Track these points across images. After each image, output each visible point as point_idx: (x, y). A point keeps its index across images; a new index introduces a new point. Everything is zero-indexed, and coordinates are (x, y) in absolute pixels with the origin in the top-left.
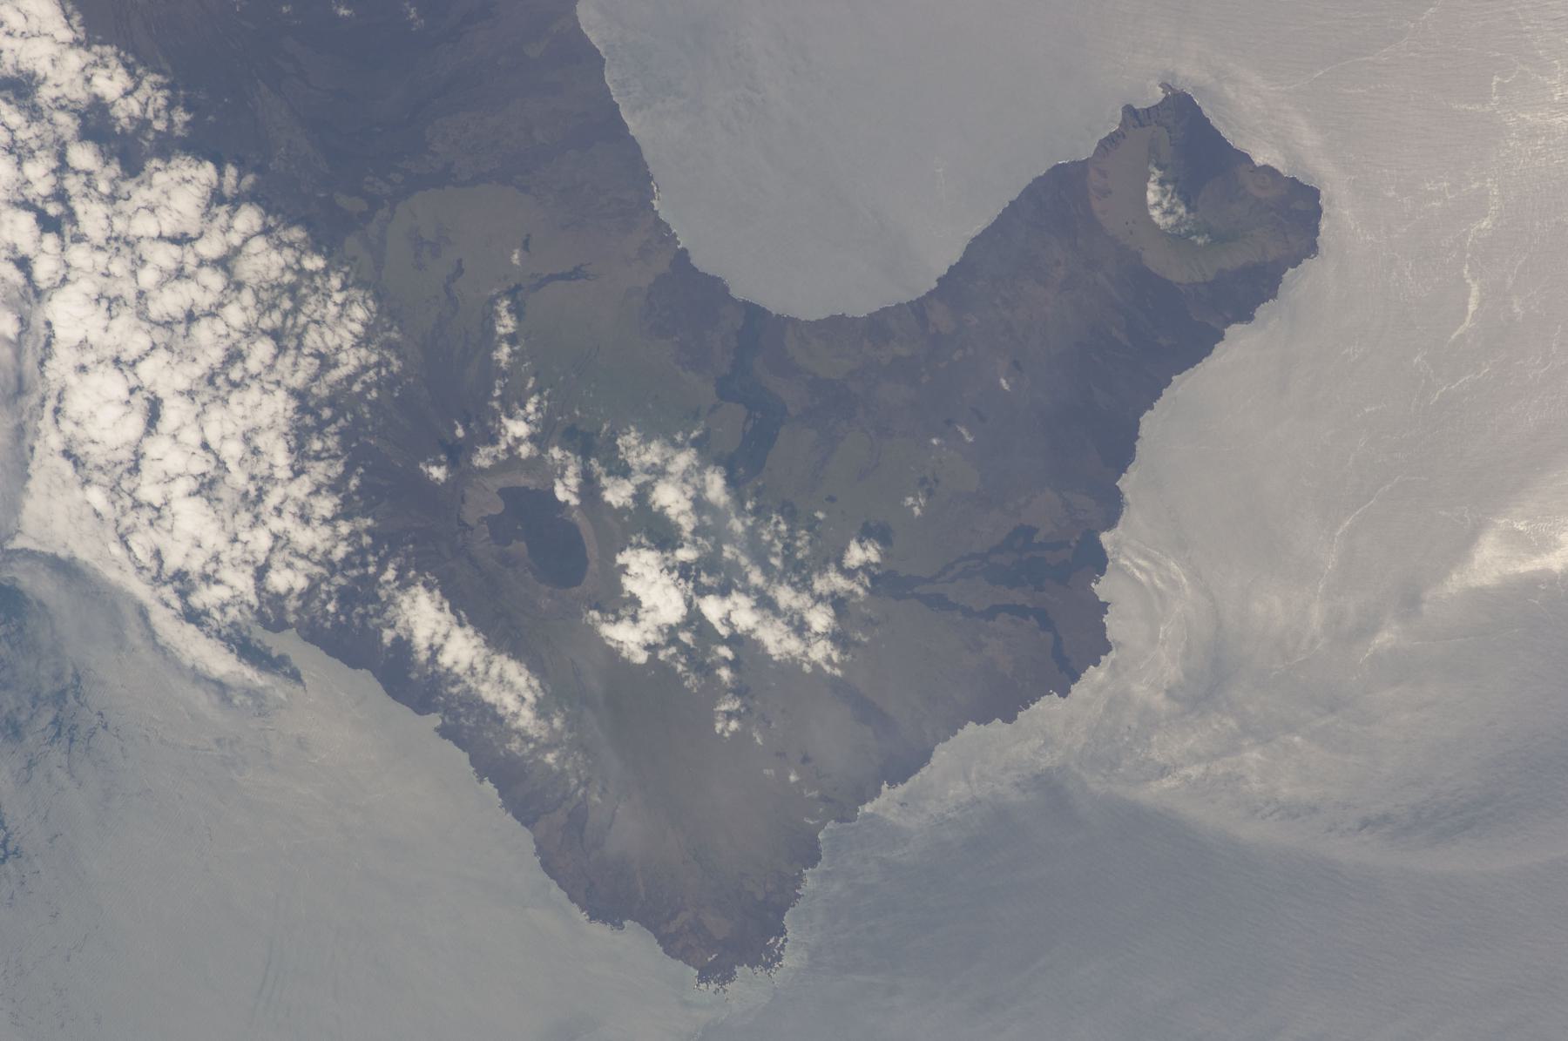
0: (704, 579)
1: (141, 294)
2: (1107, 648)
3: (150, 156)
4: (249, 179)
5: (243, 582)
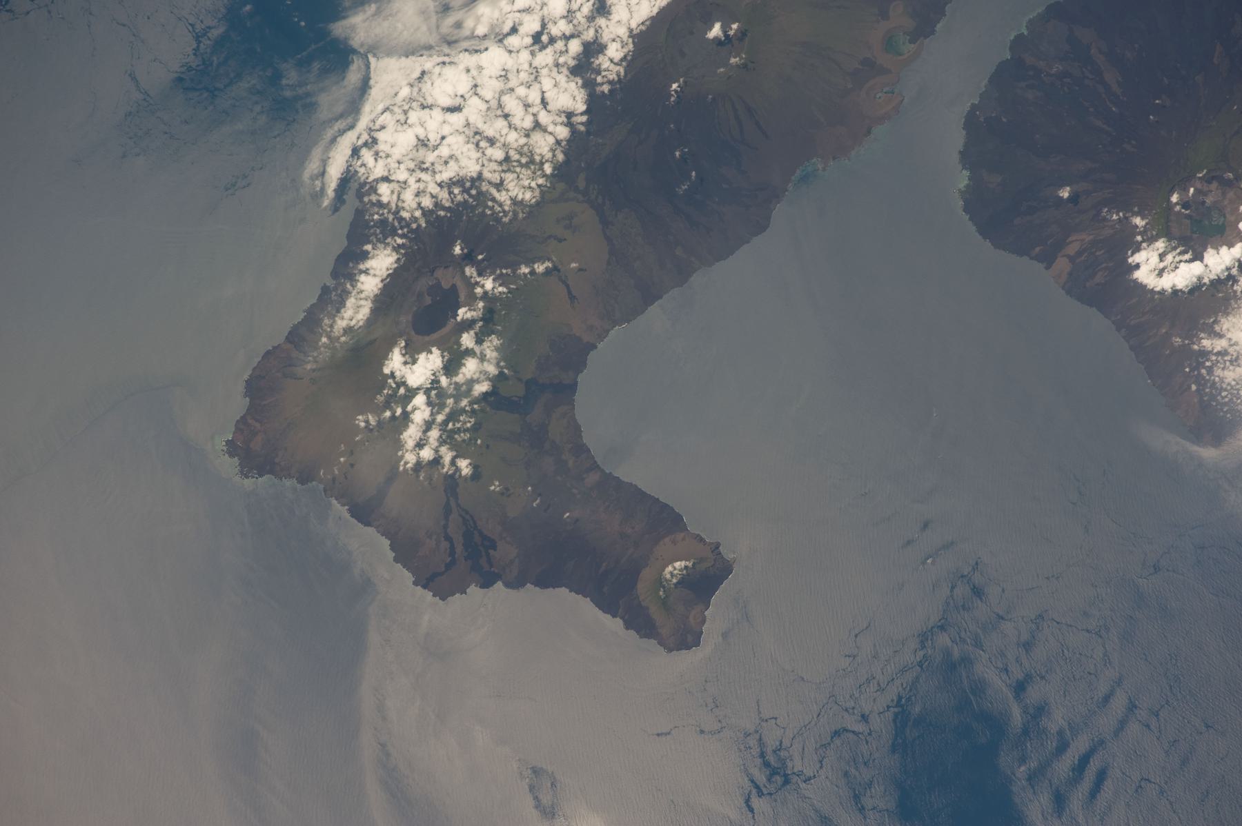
0: (434, 392)
1: (512, 90)
2: (443, 599)
3: (582, 78)
4: (582, 128)
5: (379, 171)
